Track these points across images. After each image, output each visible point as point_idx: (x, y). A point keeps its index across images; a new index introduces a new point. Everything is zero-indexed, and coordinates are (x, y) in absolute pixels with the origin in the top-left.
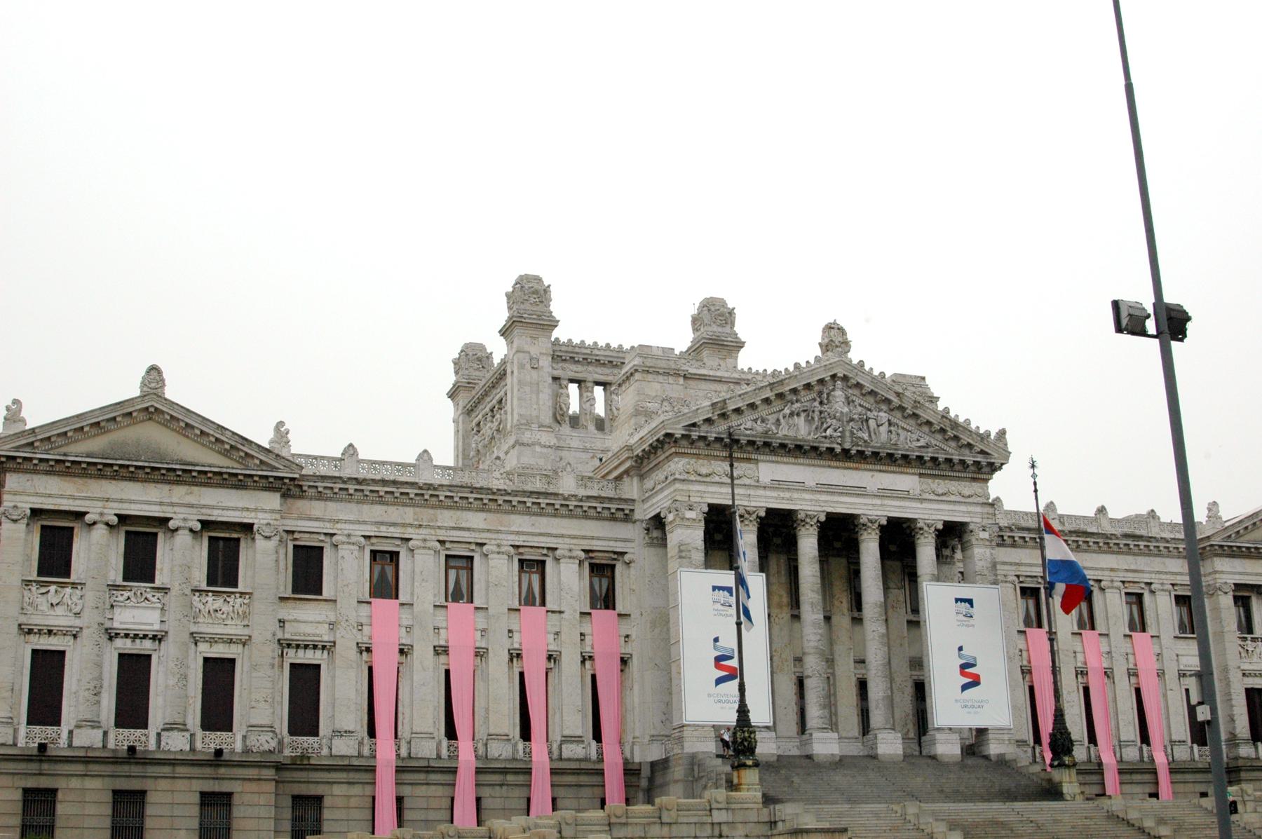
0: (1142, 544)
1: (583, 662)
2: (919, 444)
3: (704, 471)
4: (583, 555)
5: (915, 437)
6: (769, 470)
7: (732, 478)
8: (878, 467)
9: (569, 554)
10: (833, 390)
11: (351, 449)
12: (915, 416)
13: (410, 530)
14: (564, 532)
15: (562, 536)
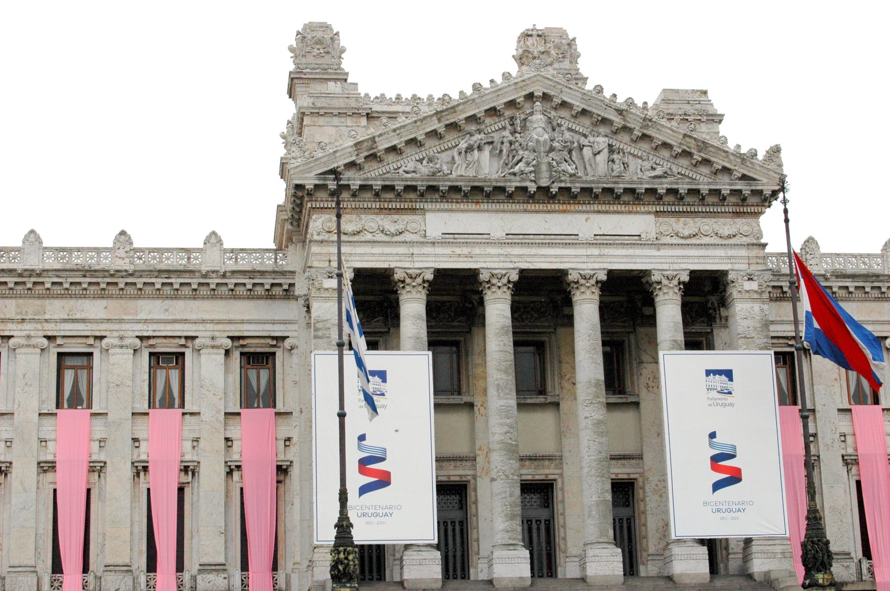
1: (230, 473)
2: (654, 173)
4: (229, 341)
5: (648, 165)
6: (439, 221)
7: (339, 232)
9: (209, 342)
10: (532, 114)
12: (644, 137)
13: (10, 326)
14: (206, 316)
15: (204, 321)
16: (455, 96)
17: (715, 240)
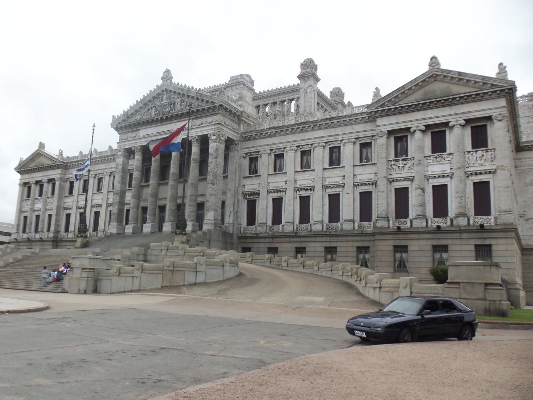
0: (335, 121)
3: (125, 137)
6: (143, 132)
8: (177, 120)
11: (81, 153)
12: (188, 96)
16: (146, 95)
17: (208, 124)
